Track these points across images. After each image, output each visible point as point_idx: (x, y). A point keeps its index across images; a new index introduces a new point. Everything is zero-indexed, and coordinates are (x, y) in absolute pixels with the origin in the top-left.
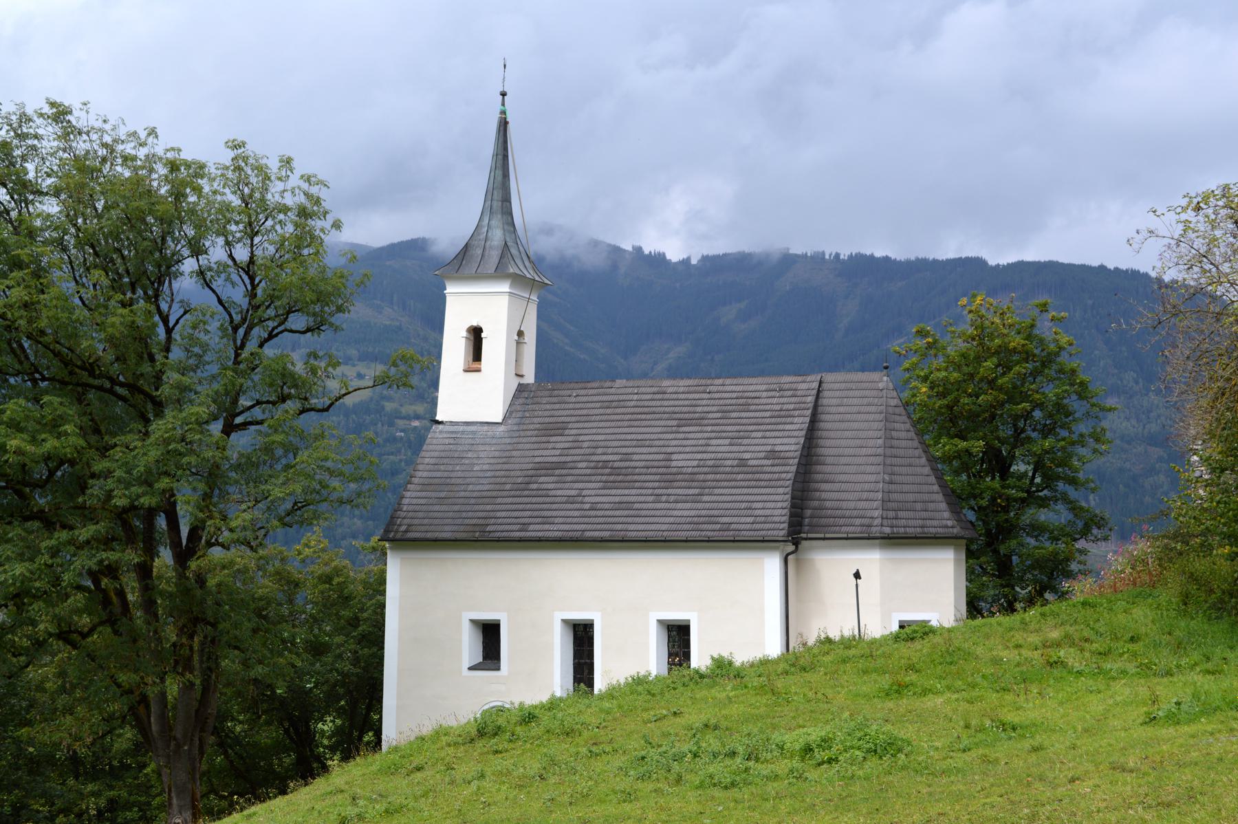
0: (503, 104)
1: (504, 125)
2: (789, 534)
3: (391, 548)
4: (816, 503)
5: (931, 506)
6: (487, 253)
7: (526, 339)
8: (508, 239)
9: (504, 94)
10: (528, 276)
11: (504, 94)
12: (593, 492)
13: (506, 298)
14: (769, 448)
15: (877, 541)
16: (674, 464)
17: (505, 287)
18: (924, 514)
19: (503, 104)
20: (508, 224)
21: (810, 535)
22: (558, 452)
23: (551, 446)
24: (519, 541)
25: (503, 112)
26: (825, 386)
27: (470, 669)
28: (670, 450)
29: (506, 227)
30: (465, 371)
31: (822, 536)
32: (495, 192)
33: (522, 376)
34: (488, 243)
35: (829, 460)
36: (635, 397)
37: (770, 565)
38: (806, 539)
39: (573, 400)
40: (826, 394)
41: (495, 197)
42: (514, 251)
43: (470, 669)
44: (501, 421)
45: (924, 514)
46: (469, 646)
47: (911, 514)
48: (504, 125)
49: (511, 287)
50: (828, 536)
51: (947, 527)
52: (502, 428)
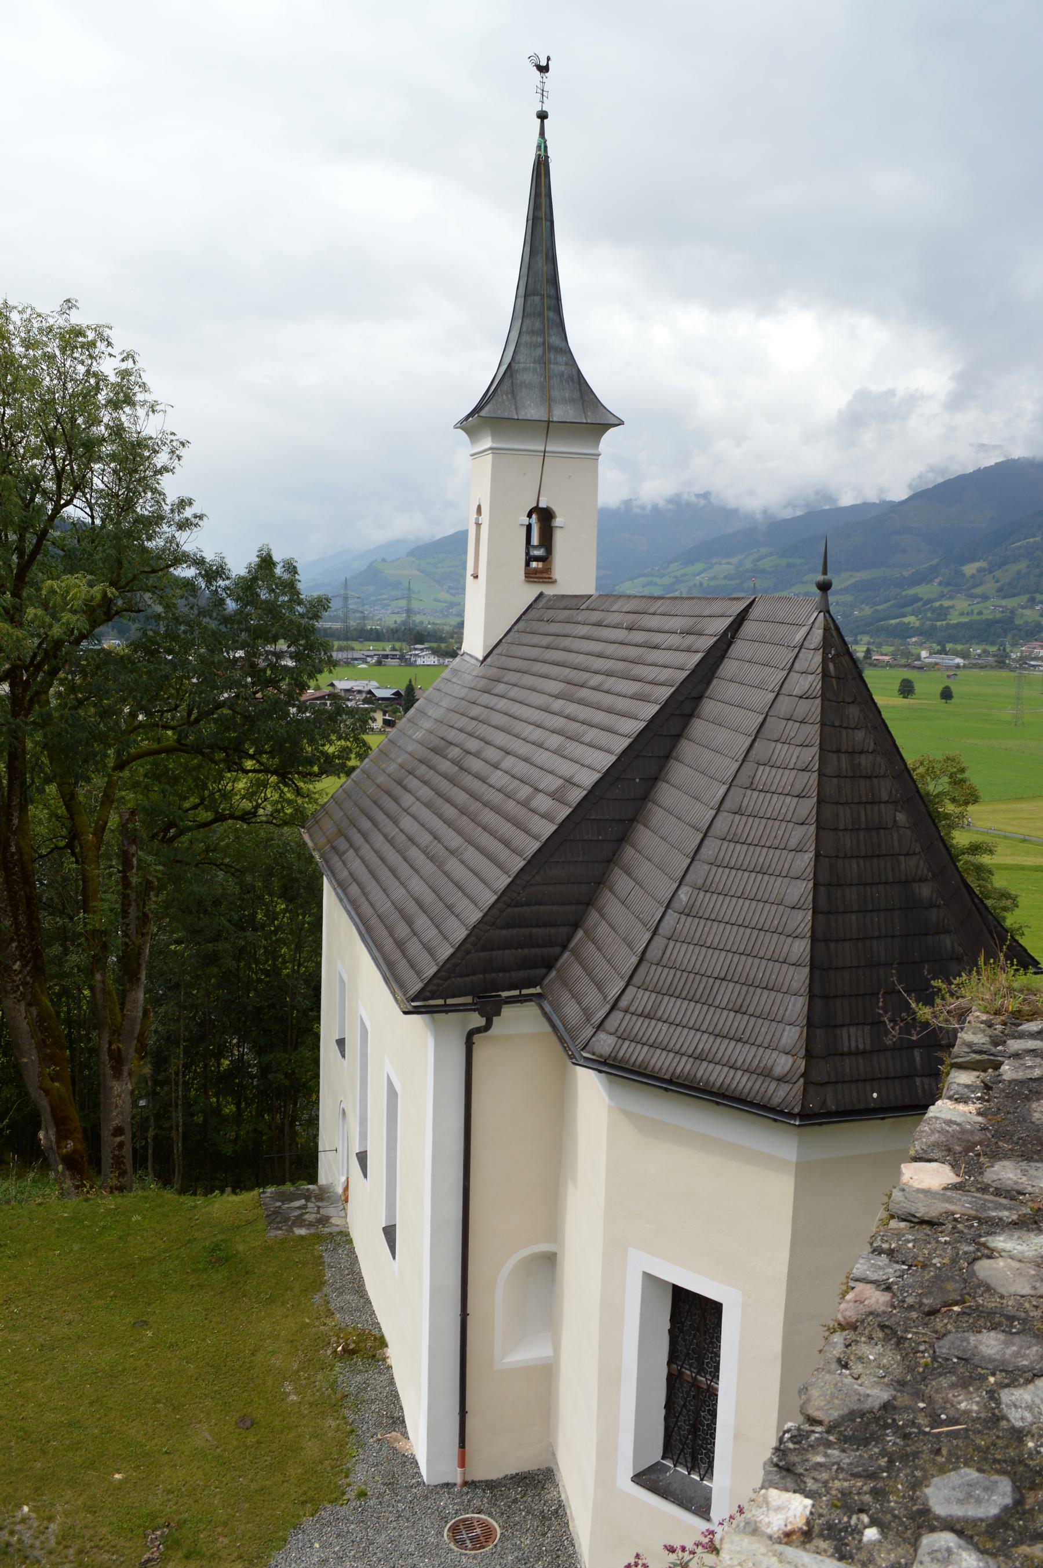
0: (542, 134)
1: (541, 169)
5: (762, 1000)
7: (558, 522)
8: (521, 358)
9: (542, 116)
11: (542, 116)
13: (489, 458)
17: (487, 443)
18: (727, 1021)
19: (542, 134)
20: (532, 332)
25: (542, 147)
26: (749, 628)
29: (526, 338)
33: (554, 582)
44: (481, 658)
45: (727, 1021)
47: (694, 1012)
48: (541, 169)
51: (767, 1073)
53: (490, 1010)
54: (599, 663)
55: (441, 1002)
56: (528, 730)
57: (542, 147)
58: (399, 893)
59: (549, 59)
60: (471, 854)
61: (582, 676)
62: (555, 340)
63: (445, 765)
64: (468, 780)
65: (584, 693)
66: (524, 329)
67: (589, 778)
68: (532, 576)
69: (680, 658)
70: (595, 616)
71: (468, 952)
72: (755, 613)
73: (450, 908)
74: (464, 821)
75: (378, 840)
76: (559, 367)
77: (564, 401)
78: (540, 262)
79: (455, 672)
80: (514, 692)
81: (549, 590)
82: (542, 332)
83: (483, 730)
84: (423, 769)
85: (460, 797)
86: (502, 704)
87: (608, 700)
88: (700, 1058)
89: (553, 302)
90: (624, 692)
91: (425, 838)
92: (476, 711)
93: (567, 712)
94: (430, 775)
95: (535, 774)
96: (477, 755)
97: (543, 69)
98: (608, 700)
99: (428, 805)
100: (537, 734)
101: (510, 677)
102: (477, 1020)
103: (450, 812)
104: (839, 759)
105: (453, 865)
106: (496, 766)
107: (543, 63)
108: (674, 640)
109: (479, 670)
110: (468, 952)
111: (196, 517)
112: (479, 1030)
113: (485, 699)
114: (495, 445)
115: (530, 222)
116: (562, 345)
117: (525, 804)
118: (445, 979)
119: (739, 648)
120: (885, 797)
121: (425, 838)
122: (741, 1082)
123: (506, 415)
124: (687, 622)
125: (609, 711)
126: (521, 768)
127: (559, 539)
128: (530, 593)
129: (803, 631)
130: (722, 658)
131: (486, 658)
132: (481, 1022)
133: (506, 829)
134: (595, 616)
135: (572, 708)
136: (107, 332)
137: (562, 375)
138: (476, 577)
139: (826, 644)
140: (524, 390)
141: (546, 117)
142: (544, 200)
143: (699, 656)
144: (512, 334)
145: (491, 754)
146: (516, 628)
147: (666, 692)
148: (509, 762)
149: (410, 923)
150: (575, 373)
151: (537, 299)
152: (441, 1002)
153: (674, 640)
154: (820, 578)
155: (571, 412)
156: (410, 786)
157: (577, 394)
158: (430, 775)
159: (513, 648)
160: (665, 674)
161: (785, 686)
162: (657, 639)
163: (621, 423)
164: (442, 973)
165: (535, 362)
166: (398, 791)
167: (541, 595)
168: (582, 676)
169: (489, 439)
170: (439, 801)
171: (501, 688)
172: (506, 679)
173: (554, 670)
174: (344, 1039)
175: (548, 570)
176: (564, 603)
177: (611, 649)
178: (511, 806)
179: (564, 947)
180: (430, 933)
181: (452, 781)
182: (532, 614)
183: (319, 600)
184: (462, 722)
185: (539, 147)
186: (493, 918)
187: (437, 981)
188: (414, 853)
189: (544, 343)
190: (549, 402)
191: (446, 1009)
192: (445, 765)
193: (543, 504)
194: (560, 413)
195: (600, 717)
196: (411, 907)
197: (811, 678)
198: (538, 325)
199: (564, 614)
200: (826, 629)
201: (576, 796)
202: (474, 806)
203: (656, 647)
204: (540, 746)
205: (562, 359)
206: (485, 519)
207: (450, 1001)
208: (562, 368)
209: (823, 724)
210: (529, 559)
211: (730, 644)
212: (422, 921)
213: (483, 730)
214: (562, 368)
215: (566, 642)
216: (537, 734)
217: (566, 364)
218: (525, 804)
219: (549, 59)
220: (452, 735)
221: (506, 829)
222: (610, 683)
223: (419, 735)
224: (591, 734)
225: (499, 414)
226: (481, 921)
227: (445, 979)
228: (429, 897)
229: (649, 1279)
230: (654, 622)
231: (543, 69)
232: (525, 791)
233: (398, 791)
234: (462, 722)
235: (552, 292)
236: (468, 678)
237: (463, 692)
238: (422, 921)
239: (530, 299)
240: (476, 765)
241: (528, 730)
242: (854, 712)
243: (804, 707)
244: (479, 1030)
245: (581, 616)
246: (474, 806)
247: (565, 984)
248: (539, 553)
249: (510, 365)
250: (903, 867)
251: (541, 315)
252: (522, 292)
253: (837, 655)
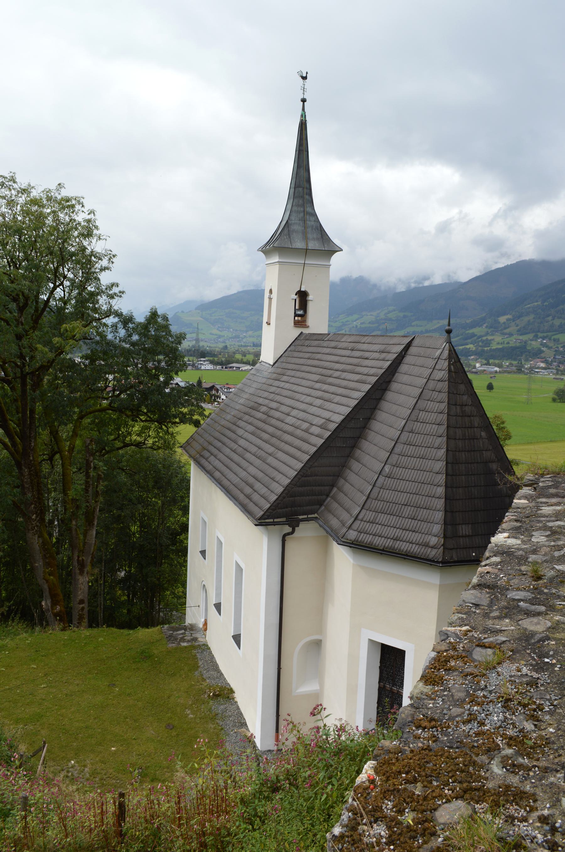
0: (303, 109)
5: (423, 513)
7: (310, 297)
8: (293, 218)
9: (304, 101)
11: (304, 101)
13: (277, 267)
16: (289, 420)
17: (276, 259)
18: (408, 523)
19: (303, 109)
20: (298, 206)
25: (303, 116)
26: (412, 350)
29: (295, 208)
33: (308, 327)
38: (303, 520)
44: (272, 364)
45: (408, 523)
47: (393, 520)
49: (279, 258)
51: (427, 545)
53: (294, 524)
54: (337, 366)
55: (272, 520)
56: (303, 398)
57: (303, 116)
58: (243, 474)
59: (307, 73)
60: (280, 454)
61: (330, 372)
62: (309, 209)
63: (259, 415)
64: (273, 421)
65: (331, 380)
66: (294, 204)
67: (339, 419)
68: (297, 324)
69: (380, 364)
70: (333, 344)
71: (284, 498)
72: (415, 343)
73: (273, 479)
74: (274, 440)
75: (227, 451)
76: (311, 223)
77: (314, 239)
78: (302, 172)
79: (258, 370)
80: (293, 380)
81: (306, 331)
82: (303, 205)
83: (278, 398)
84: (246, 417)
85: (271, 429)
86: (287, 386)
87: (344, 383)
88: (396, 539)
89: (308, 191)
90: (352, 379)
91: (254, 449)
92: (272, 389)
93: (323, 389)
94: (251, 420)
95: (310, 418)
96: (276, 410)
97: (304, 78)
98: (344, 383)
99: (253, 434)
100: (308, 399)
101: (289, 373)
102: (288, 529)
103: (266, 436)
104: (456, 408)
105: (270, 460)
106: (288, 415)
107: (304, 75)
108: (376, 355)
109: (271, 370)
110: (284, 498)
111: (120, 292)
112: (289, 534)
113: (277, 383)
114: (280, 260)
115: (297, 152)
116: (313, 212)
117: (306, 431)
118: (274, 510)
119: (408, 359)
120: (476, 425)
121: (254, 449)
122: (415, 549)
123: (286, 246)
124: (382, 347)
125: (345, 388)
126: (301, 415)
127: (311, 307)
128: (296, 332)
129: (439, 352)
130: (400, 363)
131: (274, 364)
132: (289, 529)
133: (298, 442)
134: (333, 344)
135: (325, 387)
136: (82, 200)
137: (312, 227)
138: (268, 324)
139: (450, 357)
140: (294, 234)
141: (306, 101)
142: (304, 141)
143: (389, 363)
144: (288, 206)
145: (284, 409)
146: (289, 349)
147: (374, 379)
148: (294, 412)
149: (252, 487)
150: (319, 226)
151: (301, 189)
152: (272, 520)
153: (376, 355)
154: (447, 328)
155: (317, 245)
156: (240, 426)
157: (320, 236)
158: (251, 420)
159: (290, 359)
160: (373, 371)
161: (432, 376)
162: (367, 354)
163: (342, 250)
164: (272, 507)
165: (299, 220)
166: (234, 428)
167: (302, 333)
168: (330, 372)
169: (278, 257)
170: (258, 432)
171: (285, 378)
172: (287, 374)
173: (314, 370)
174: (205, 551)
175: (305, 321)
176: (315, 338)
177: (343, 359)
178: (298, 432)
179: (328, 496)
180: (264, 490)
181: (264, 422)
182: (297, 342)
183: (181, 334)
184: (266, 394)
185: (302, 116)
186: (295, 482)
187: (270, 511)
188: (248, 455)
189: (304, 211)
190: (306, 238)
191: (274, 524)
192: (259, 415)
193: (303, 289)
194: (312, 245)
195: (340, 391)
196: (251, 480)
197: (443, 372)
198: (301, 201)
199: (316, 343)
200: (450, 351)
201: (333, 426)
202: (279, 433)
203: (367, 359)
204: (311, 405)
205: (312, 219)
206: (274, 296)
207: (276, 520)
208: (313, 223)
209: (449, 393)
210: (296, 315)
211: (403, 357)
212: (258, 486)
213: (278, 398)
214: (313, 223)
215: (319, 356)
216: (308, 399)
217: (315, 221)
218: (306, 431)
219: (307, 73)
220: (261, 401)
221: (298, 442)
222: (344, 375)
223: (242, 401)
224: (337, 399)
225: (283, 245)
226: (290, 484)
227: (274, 510)
228: (260, 475)
229: (371, 642)
230: (365, 347)
232: (305, 426)
233: (234, 428)
234: (266, 394)
235: (308, 186)
236: (266, 374)
237: (264, 380)
238: (258, 486)
239: (297, 189)
240: (277, 414)
241: (303, 398)
242: (462, 387)
243: (440, 385)
244: (289, 534)
245: (325, 344)
246: (279, 433)
247: (330, 511)
248: (301, 312)
249: (287, 221)
250: (484, 456)
251: (303, 197)
252: (293, 186)
253: (455, 362)
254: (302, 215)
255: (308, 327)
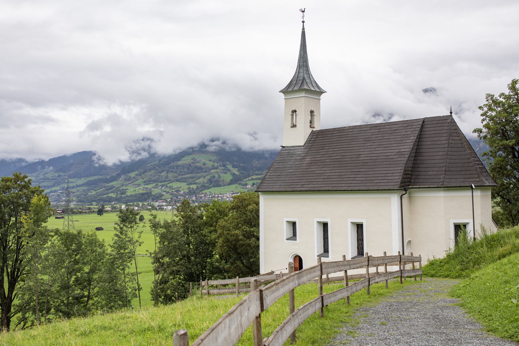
0: (303, 26)
2: (400, 187)
3: (261, 194)
4: (417, 173)
6: (297, 82)
7: (315, 114)
9: (303, 22)
10: (312, 89)
11: (303, 22)
12: (329, 171)
14: (398, 151)
15: (442, 188)
17: (303, 94)
19: (303, 26)
21: (414, 187)
22: (320, 156)
23: (318, 154)
24: (300, 191)
25: (303, 29)
27: (287, 239)
28: (360, 153)
30: (291, 127)
31: (418, 187)
32: (301, 59)
34: (298, 79)
35: (425, 154)
36: (351, 133)
37: (394, 199)
39: (329, 135)
40: (425, 126)
41: (301, 61)
42: (308, 81)
43: (287, 239)
46: (286, 231)
50: (421, 187)
52: (303, 148)
57: (303, 29)
59: (305, 9)
68: (311, 127)
81: (314, 130)
97: (303, 12)
107: (303, 10)
128: (310, 130)
132: (405, 192)
163: (326, 92)
185: (303, 29)
198: (307, 69)
219: (305, 9)
231: (303, 12)
244: (404, 194)
254: (308, 75)
255: (314, 128)
